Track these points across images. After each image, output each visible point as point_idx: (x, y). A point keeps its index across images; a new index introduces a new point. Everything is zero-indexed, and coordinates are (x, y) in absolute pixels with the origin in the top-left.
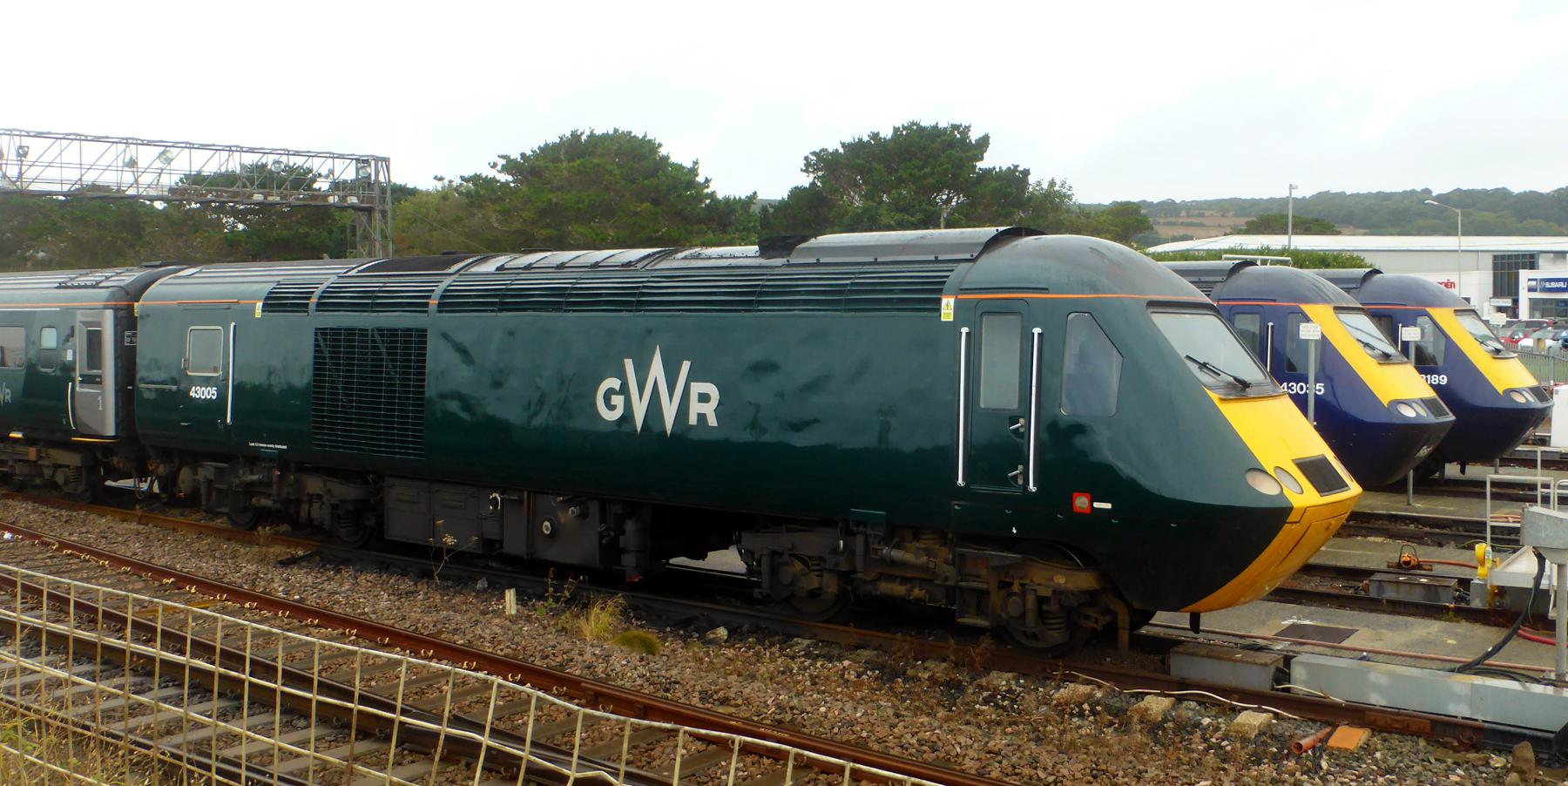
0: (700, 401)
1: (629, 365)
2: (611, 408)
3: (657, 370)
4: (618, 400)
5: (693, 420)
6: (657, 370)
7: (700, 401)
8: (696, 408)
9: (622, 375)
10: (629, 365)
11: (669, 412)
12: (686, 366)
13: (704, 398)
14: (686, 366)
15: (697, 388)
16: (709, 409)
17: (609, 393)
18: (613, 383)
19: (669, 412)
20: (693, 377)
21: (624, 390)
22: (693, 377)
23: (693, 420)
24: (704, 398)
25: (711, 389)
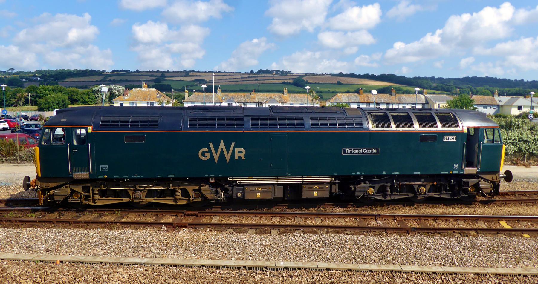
0: (238, 153)
1: (211, 144)
2: (206, 156)
3: (222, 145)
4: (208, 155)
5: (236, 158)
6: (222, 145)
7: (238, 153)
8: (237, 155)
9: (209, 147)
10: (211, 144)
11: (228, 157)
12: (233, 144)
13: (240, 152)
14: (233, 144)
15: (237, 150)
16: (242, 155)
17: (205, 152)
18: (207, 150)
19: (228, 157)
21: (210, 151)
22: (235, 147)
23: (236, 158)
24: (240, 152)
25: (243, 150)
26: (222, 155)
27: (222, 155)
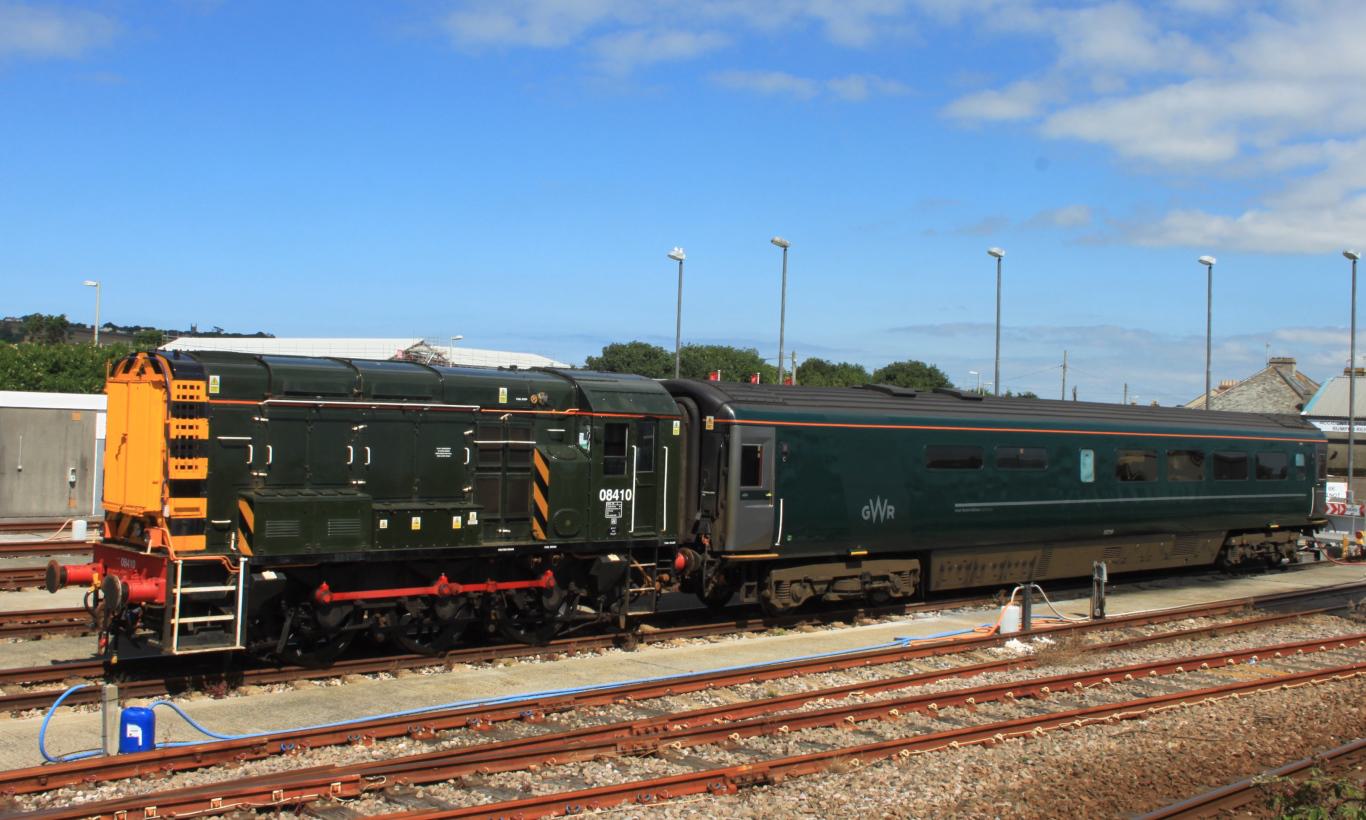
1: (871, 501)
2: (866, 515)
3: (878, 504)
4: (868, 512)
6: (878, 504)
8: (889, 513)
10: (871, 501)
11: (882, 515)
12: (886, 501)
13: (891, 510)
14: (886, 501)
15: (890, 507)
16: (891, 514)
18: (866, 507)
19: (882, 515)
20: (889, 504)
21: (870, 509)
22: (889, 504)
25: (892, 508)
26: (878, 516)
27: (878, 516)
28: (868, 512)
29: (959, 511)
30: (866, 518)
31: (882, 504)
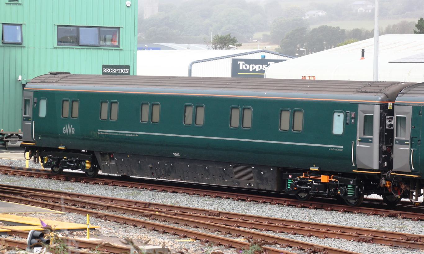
1: (66, 125)
2: (64, 131)
4: (65, 130)
5: (72, 133)
10: (66, 125)
11: (70, 132)
12: (72, 125)
13: (73, 130)
14: (72, 125)
15: (73, 129)
16: (73, 132)
17: (64, 129)
18: (64, 128)
20: (72, 127)
21: (66, 129)
22: (72, 127)
23: (72, 133)
24: (73, 130)
28: (65, 130)
29: (99, 133)
30: (64, 133)
31: (70, 128)
